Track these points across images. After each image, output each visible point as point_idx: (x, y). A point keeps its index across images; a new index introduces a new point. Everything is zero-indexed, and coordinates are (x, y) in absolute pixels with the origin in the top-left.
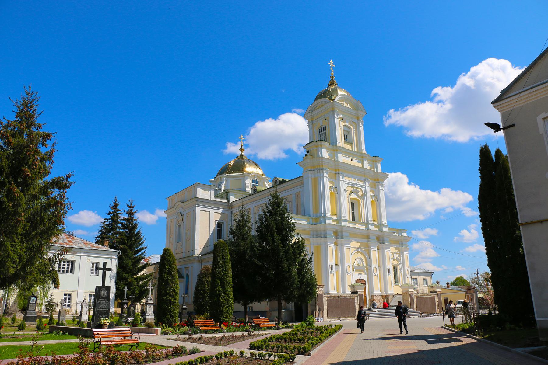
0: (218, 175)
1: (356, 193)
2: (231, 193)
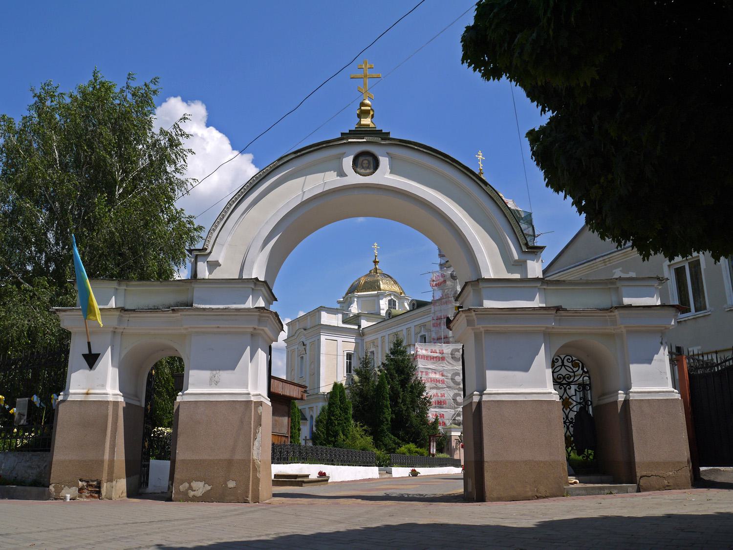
0: (347, 294)
2: (362, 317)
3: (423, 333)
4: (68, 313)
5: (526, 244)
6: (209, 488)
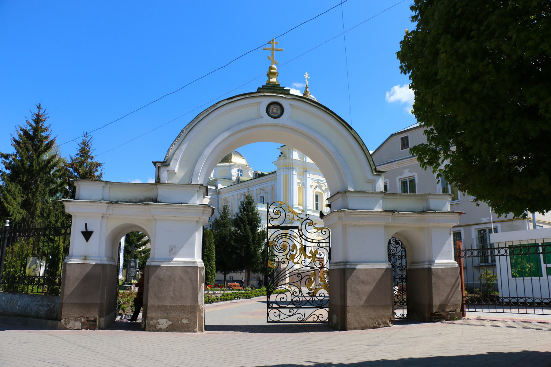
1: (320, 187)
2: (219, 181)
3: (262, 195)
4: (72, 203)
5: (375, 169)
6: (171, 323)
